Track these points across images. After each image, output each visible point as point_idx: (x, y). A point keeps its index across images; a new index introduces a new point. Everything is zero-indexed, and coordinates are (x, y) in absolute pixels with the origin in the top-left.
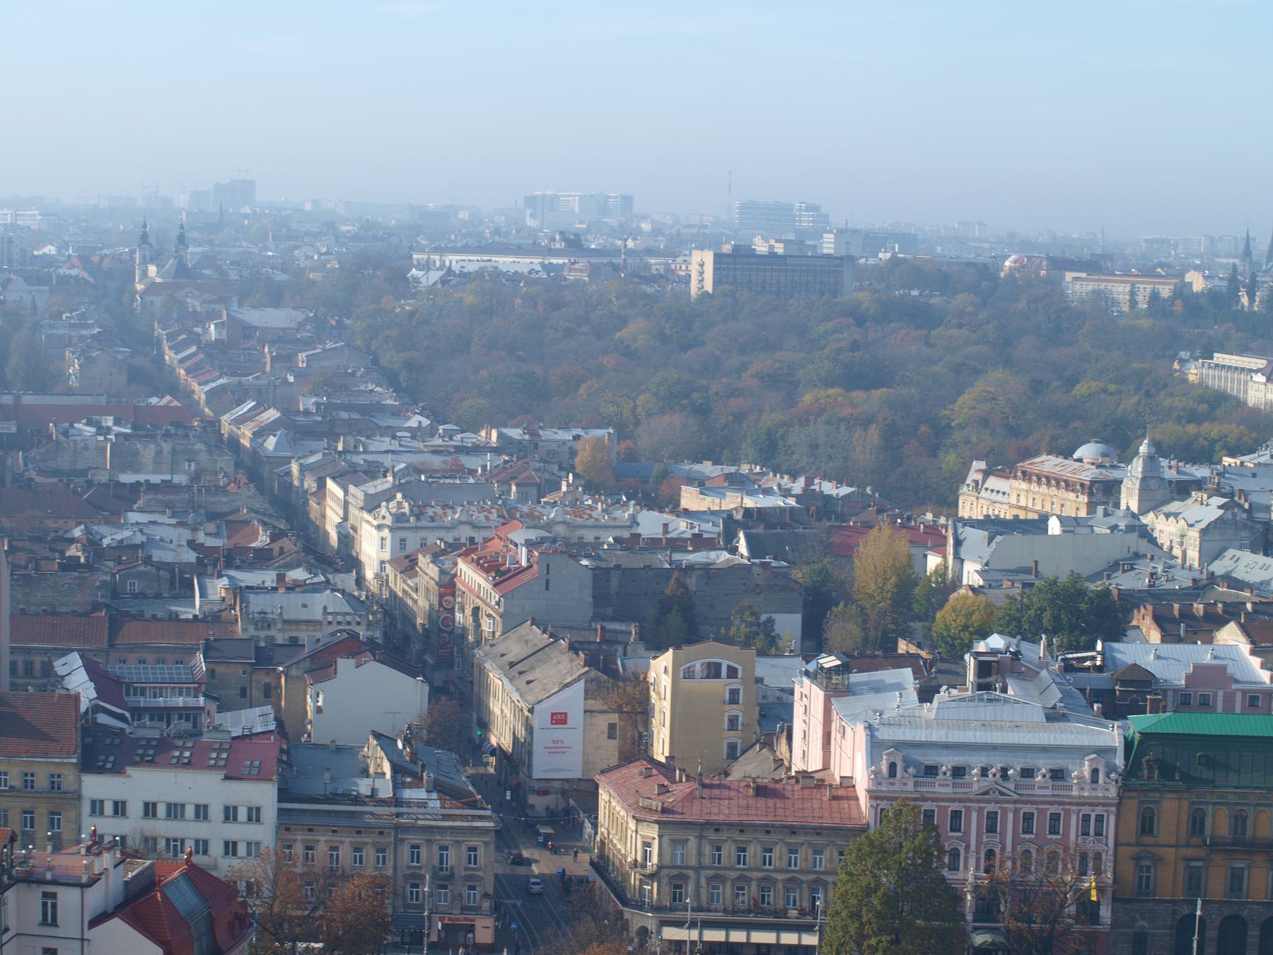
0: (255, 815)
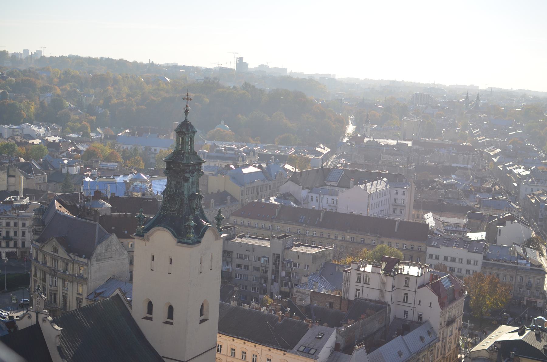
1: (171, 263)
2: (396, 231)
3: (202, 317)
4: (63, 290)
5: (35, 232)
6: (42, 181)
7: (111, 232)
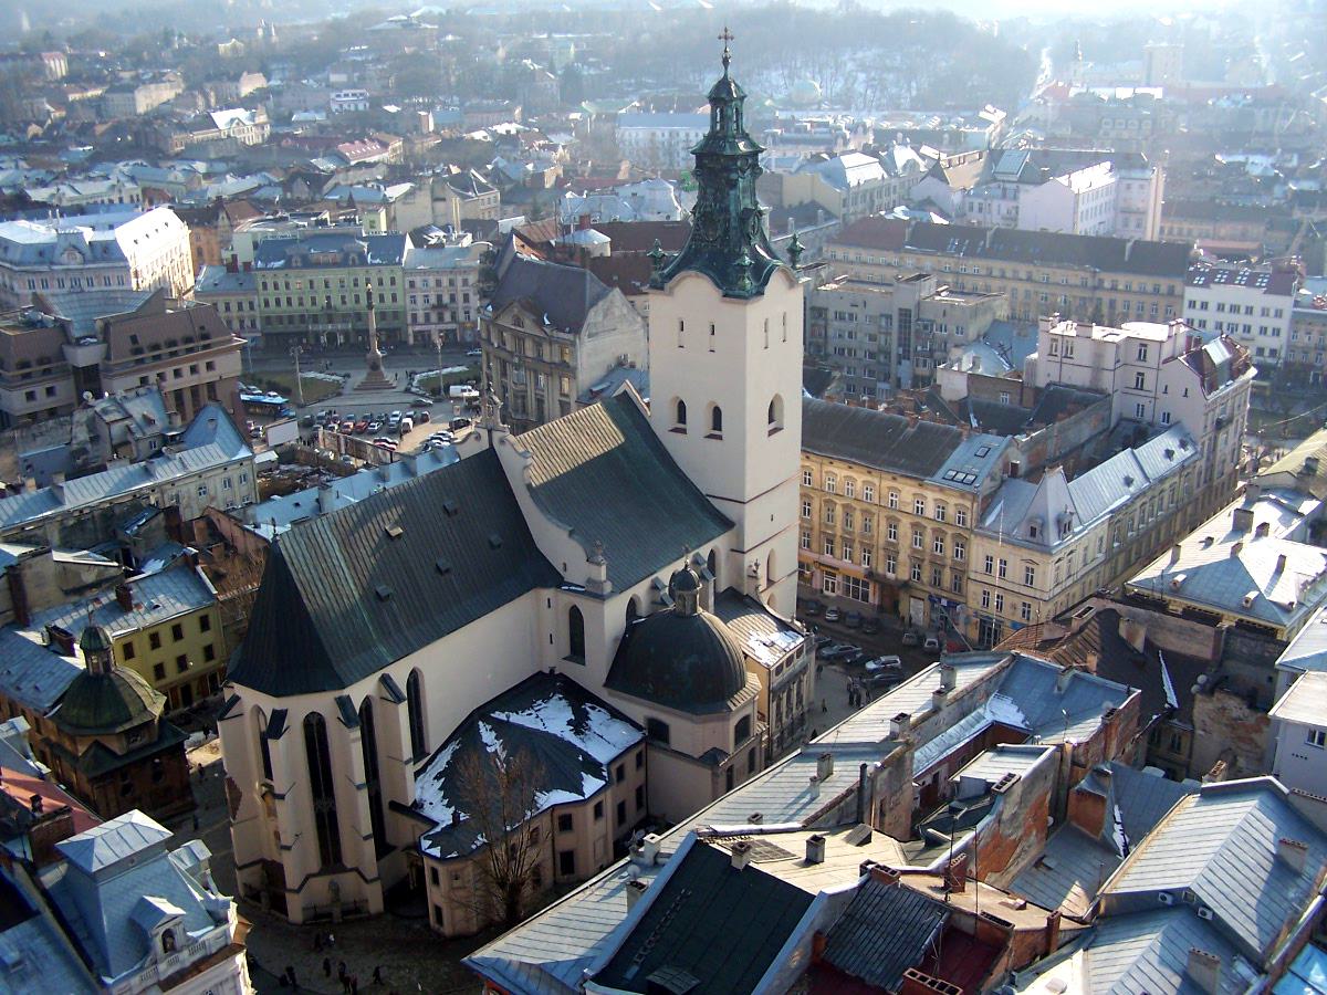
0: (1279, 314)
1: (713, 333)
2: (1126, 259)
3: (773, 425)
4: (536, 389)
5: (483, 294)
6: (493, 204)
7: (611, 284)
